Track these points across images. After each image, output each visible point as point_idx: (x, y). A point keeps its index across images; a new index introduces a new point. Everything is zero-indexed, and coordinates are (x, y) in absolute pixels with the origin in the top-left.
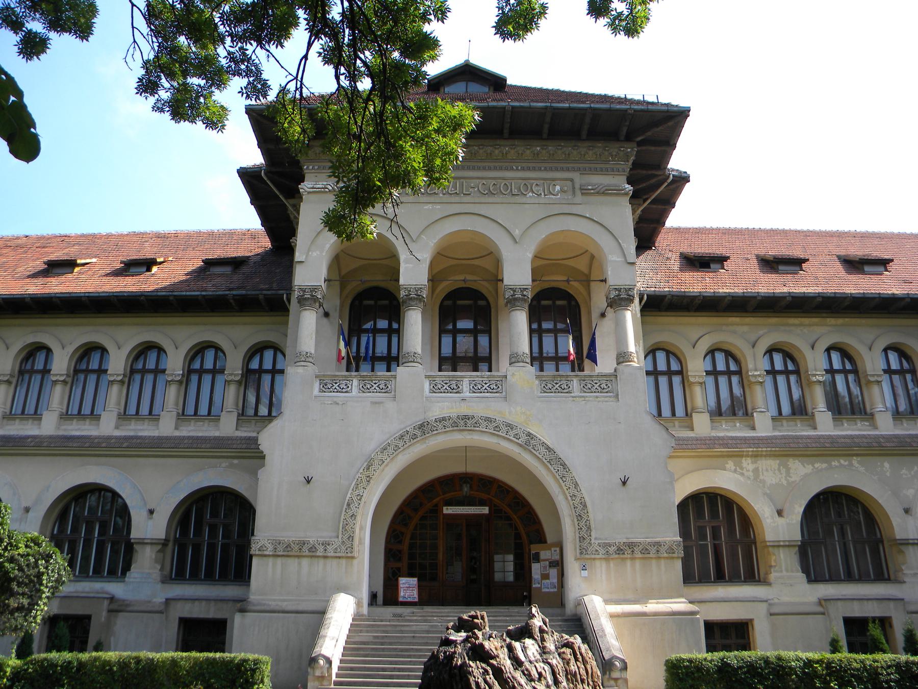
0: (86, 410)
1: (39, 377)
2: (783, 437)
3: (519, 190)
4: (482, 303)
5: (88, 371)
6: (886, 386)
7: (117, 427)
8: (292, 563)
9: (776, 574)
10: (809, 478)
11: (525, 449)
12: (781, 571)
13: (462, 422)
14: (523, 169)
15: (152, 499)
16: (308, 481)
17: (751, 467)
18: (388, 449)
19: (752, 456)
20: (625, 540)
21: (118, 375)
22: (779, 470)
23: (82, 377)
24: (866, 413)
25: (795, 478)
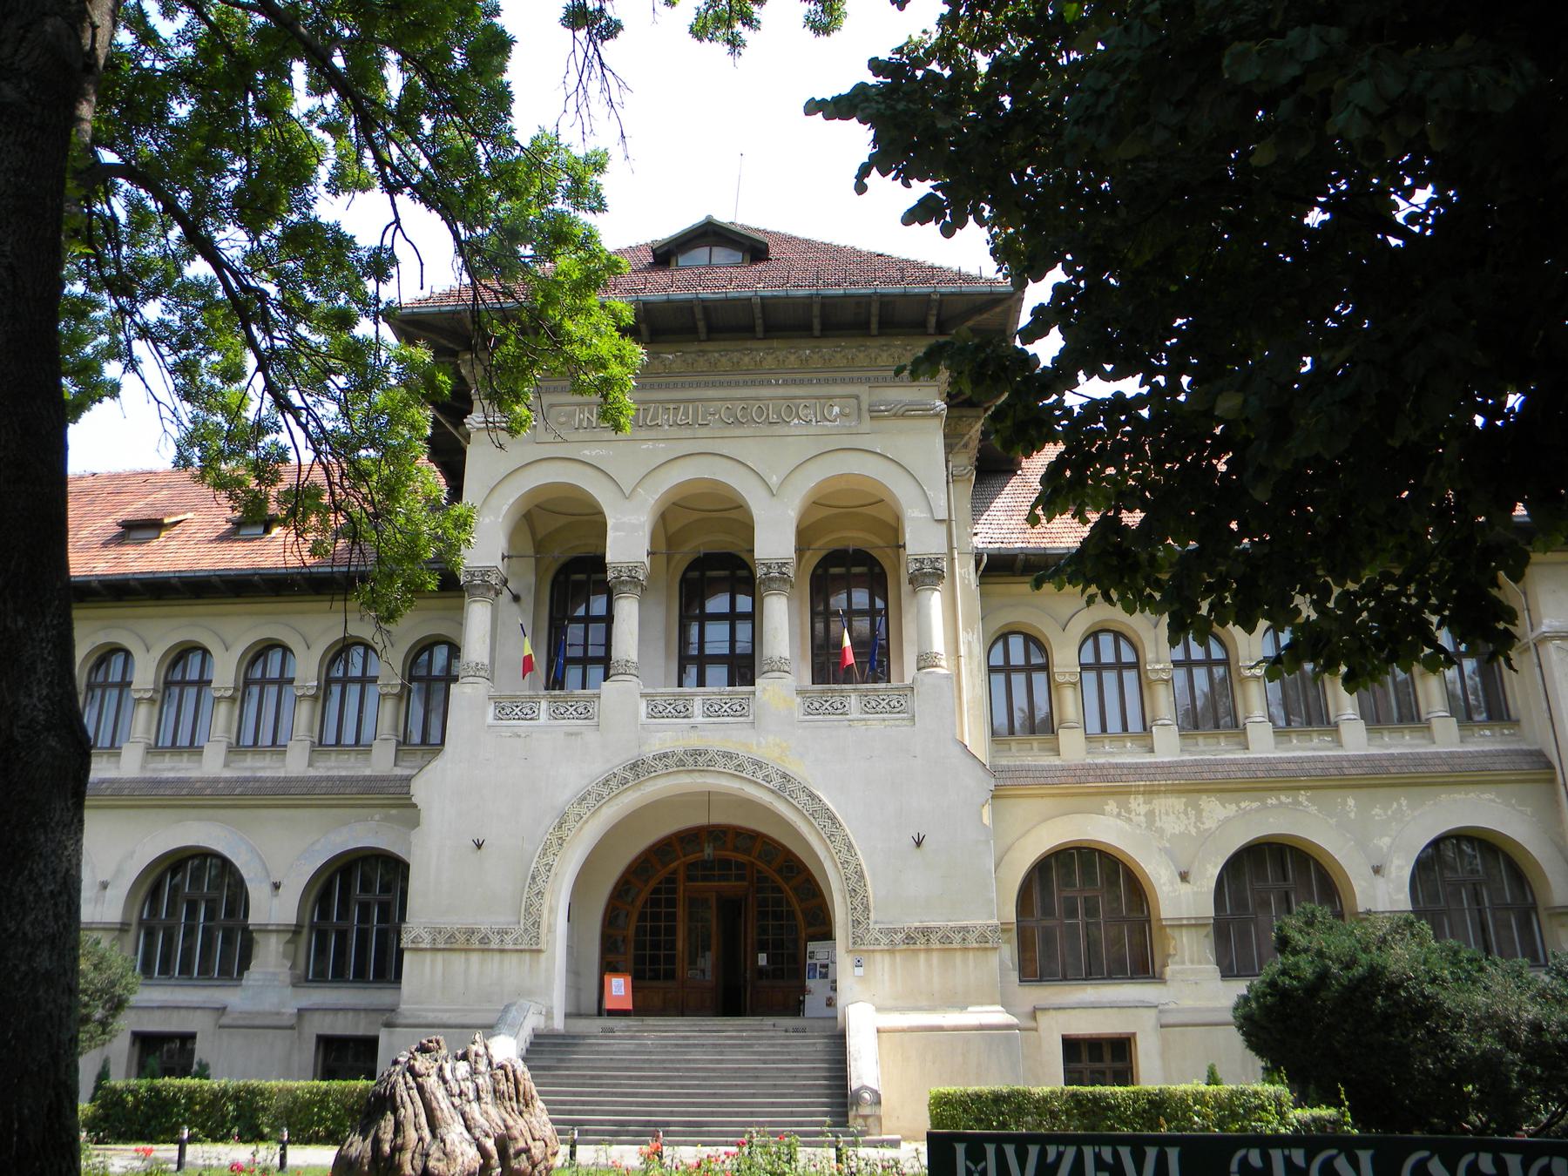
0: (184, 740)
1: (115, 692)
2: (1196, 763)
3: (779, 415)
4: (742, 573)
5: (184, 683)
7: (226, 765)
8: (458, 960)
9: (1177, 967)
10: (1234, 824)
11: (780, 797)
12: (1183, 963)
13: (691, 760)
14: (786, 383)
15: (278, 869)
16: (479, 846)
17: (1143, 809)
18: (589, 799)
19: (1144, 793)
20: (917, 924)
21: (227, 689)
22: (1186, 813)
23: (176, 691)
24: (1329, 723)
25: (1210, 824)
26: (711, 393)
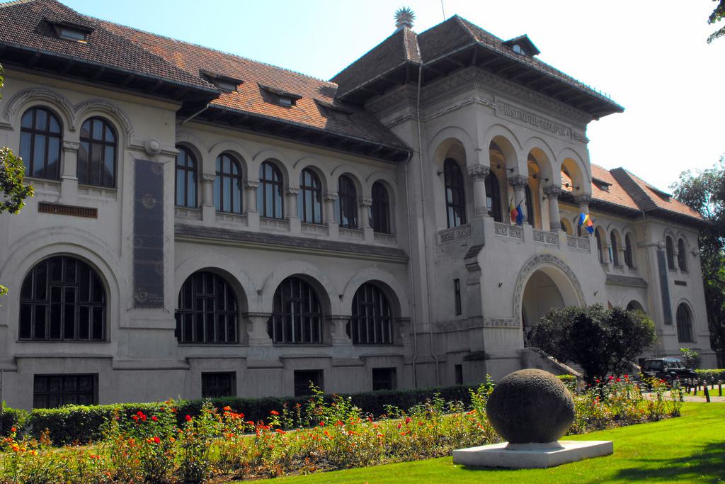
6: (260, 191)
26: (538, 114)
